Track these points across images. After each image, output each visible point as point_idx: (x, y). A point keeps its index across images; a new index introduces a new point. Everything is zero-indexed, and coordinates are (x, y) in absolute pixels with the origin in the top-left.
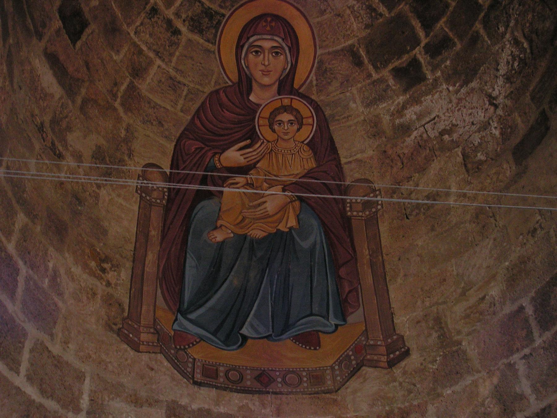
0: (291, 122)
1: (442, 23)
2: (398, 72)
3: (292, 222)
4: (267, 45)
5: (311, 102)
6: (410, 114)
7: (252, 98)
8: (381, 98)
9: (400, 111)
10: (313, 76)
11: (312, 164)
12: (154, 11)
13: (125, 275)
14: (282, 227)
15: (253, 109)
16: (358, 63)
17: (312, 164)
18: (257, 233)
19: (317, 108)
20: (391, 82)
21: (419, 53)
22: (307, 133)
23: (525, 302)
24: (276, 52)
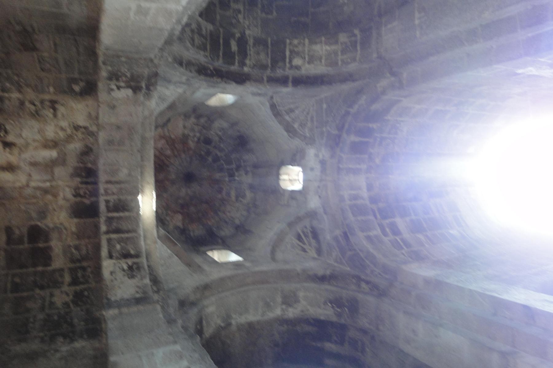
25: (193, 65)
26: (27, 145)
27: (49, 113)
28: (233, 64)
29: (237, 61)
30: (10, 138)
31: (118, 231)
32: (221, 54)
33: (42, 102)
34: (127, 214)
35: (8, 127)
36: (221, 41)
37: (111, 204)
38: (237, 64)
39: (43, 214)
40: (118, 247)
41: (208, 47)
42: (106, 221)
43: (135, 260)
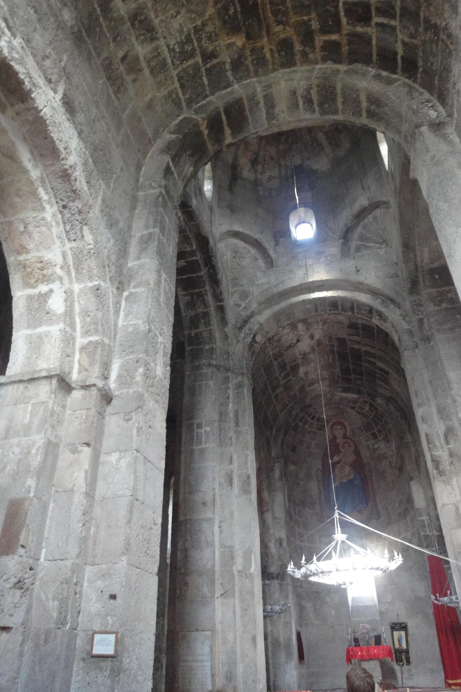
0: (348, 446)
1: (379, 426)
2: (371, 434)
3: (352, 476)
4: (338, 428)
5: (352, 440)
6: (376, 446)
7: (337, 441)
8: (369, 440)
9: (374, 445)
10: (351, 434)
11: (355, 458)
12: (309, 432)
13: (318, 505)
14: (350, 478)
15: (338, 444)
16: (362, 431)
17: (355, 458)
18: (345, 481)
19: (354, 442)
20: (370, 436)
21: (375, 430)
22: (352, 449)
23: (402, 510)
24: (341, 429)
25: (214, 291)
26: (297, 335)
27: (276, 338)
28: (197, 261)
29: (192, 259)
30: (295, 341)
31: (352, 309)
32: (196, 275)
33: (270, 343)
34: (339, 303)
35: (288, 344)
36: (184, 277)
37: (332, 309)
38: (195, 258)
39: (340, 323)
40: (363, 312)
41: (198, 291)
42: (344, 311)
43: (374, 311)
